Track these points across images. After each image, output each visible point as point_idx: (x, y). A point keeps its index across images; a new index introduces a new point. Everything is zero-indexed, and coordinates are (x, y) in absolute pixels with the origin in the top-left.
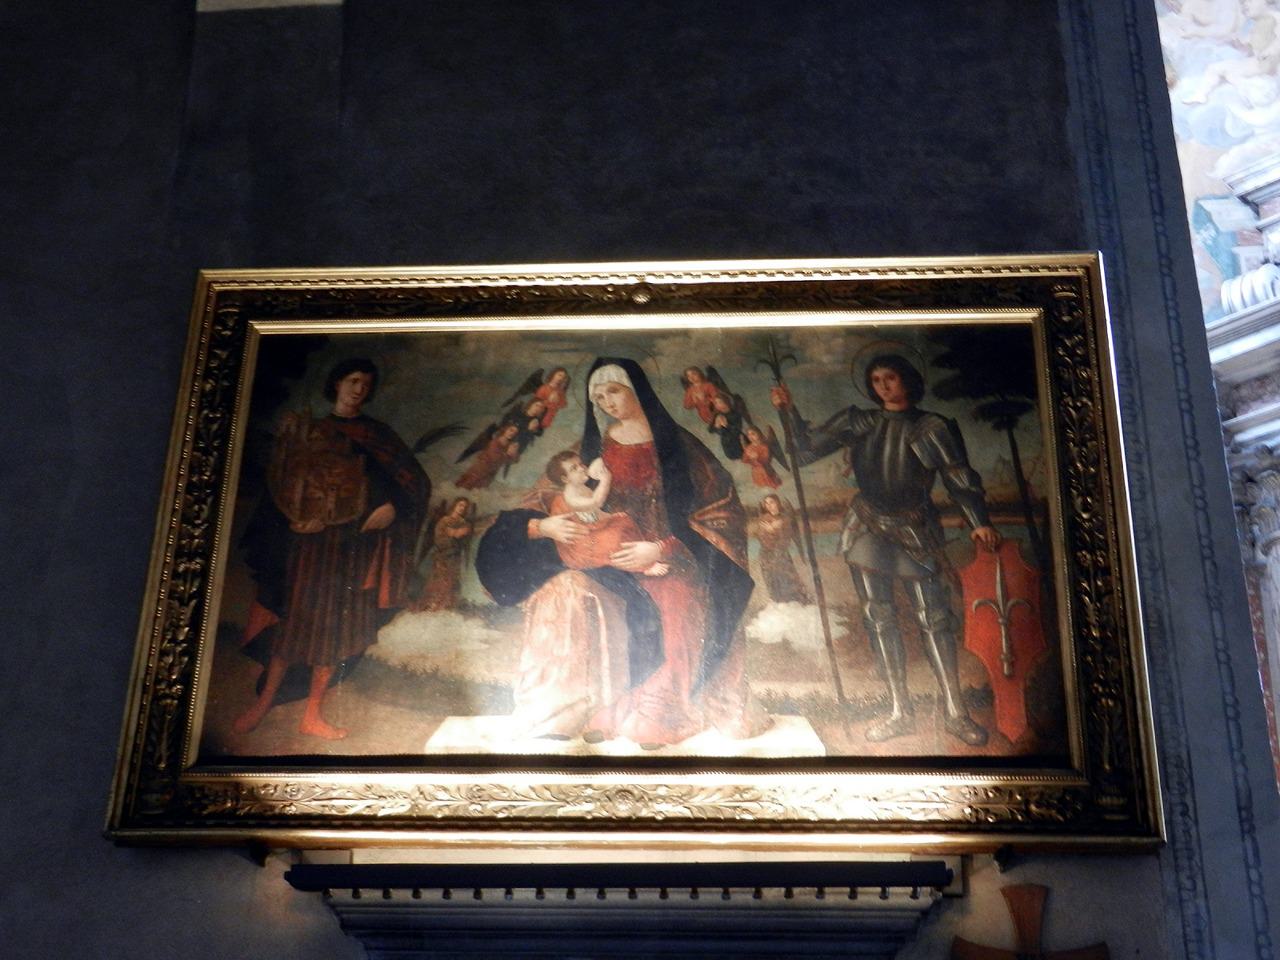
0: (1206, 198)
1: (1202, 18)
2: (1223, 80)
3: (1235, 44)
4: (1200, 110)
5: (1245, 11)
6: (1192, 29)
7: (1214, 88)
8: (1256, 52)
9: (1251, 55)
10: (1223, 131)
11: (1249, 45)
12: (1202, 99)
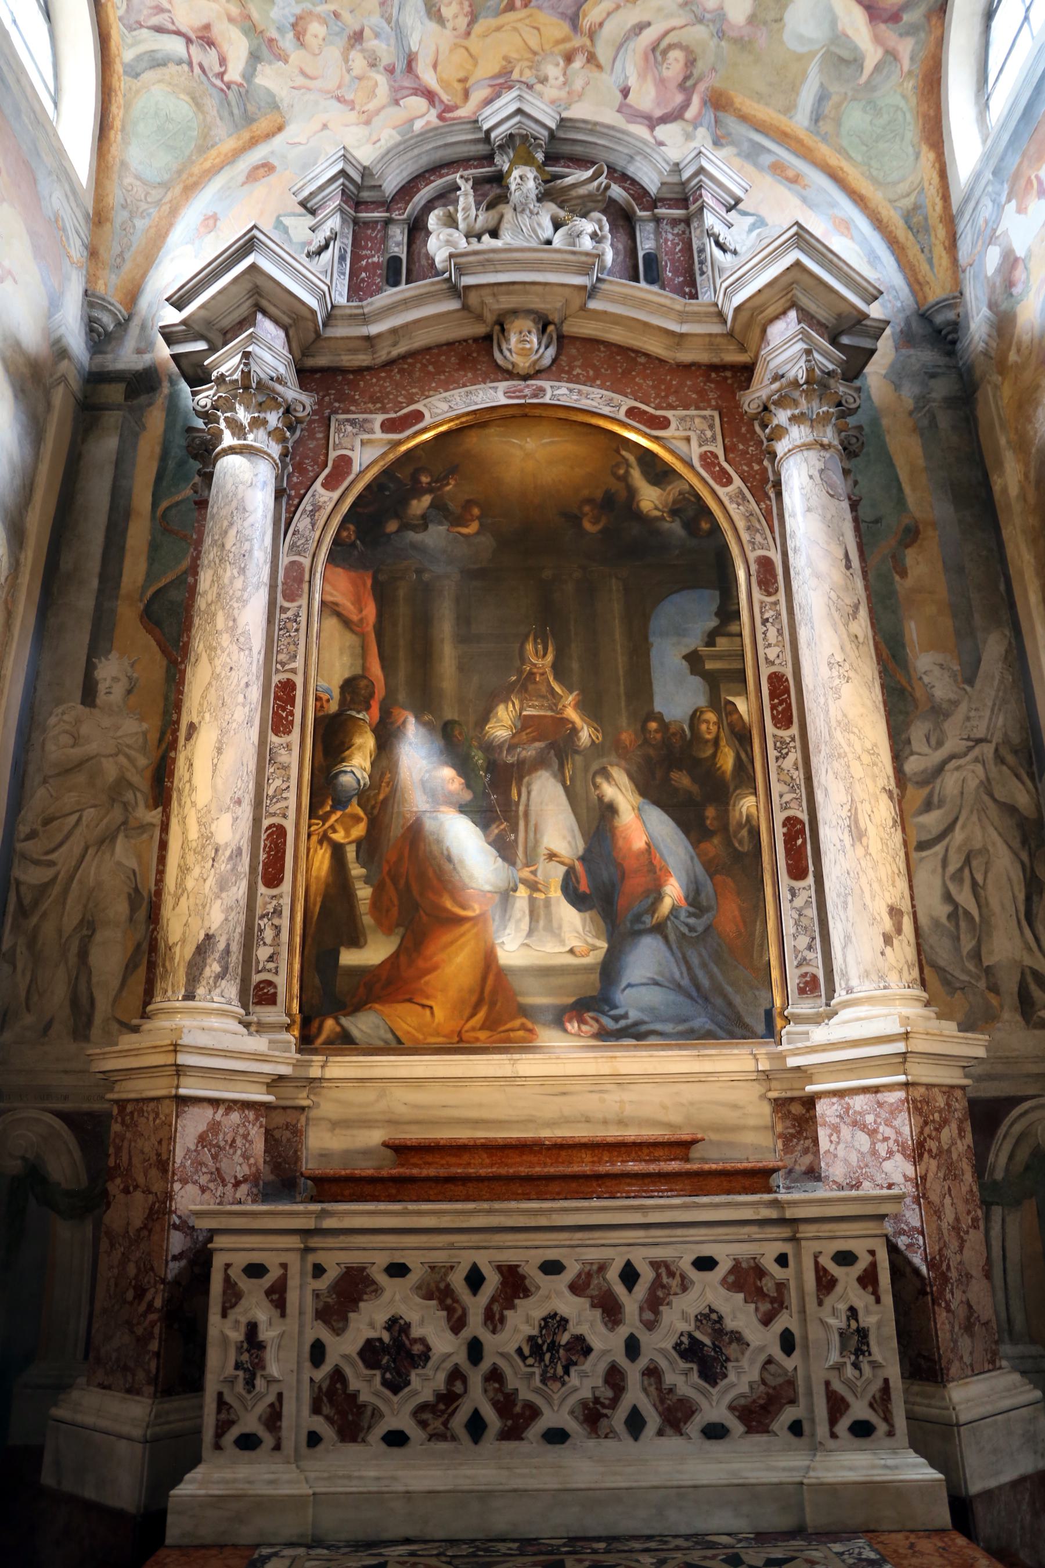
2: (325, 126)
3: (340, 99)
5: (349, 71)
6: (300, 81)
7: (316, 133)
8: (357, 107)
9: (353, 109)
11: (353, 102)
12: (304, 141)
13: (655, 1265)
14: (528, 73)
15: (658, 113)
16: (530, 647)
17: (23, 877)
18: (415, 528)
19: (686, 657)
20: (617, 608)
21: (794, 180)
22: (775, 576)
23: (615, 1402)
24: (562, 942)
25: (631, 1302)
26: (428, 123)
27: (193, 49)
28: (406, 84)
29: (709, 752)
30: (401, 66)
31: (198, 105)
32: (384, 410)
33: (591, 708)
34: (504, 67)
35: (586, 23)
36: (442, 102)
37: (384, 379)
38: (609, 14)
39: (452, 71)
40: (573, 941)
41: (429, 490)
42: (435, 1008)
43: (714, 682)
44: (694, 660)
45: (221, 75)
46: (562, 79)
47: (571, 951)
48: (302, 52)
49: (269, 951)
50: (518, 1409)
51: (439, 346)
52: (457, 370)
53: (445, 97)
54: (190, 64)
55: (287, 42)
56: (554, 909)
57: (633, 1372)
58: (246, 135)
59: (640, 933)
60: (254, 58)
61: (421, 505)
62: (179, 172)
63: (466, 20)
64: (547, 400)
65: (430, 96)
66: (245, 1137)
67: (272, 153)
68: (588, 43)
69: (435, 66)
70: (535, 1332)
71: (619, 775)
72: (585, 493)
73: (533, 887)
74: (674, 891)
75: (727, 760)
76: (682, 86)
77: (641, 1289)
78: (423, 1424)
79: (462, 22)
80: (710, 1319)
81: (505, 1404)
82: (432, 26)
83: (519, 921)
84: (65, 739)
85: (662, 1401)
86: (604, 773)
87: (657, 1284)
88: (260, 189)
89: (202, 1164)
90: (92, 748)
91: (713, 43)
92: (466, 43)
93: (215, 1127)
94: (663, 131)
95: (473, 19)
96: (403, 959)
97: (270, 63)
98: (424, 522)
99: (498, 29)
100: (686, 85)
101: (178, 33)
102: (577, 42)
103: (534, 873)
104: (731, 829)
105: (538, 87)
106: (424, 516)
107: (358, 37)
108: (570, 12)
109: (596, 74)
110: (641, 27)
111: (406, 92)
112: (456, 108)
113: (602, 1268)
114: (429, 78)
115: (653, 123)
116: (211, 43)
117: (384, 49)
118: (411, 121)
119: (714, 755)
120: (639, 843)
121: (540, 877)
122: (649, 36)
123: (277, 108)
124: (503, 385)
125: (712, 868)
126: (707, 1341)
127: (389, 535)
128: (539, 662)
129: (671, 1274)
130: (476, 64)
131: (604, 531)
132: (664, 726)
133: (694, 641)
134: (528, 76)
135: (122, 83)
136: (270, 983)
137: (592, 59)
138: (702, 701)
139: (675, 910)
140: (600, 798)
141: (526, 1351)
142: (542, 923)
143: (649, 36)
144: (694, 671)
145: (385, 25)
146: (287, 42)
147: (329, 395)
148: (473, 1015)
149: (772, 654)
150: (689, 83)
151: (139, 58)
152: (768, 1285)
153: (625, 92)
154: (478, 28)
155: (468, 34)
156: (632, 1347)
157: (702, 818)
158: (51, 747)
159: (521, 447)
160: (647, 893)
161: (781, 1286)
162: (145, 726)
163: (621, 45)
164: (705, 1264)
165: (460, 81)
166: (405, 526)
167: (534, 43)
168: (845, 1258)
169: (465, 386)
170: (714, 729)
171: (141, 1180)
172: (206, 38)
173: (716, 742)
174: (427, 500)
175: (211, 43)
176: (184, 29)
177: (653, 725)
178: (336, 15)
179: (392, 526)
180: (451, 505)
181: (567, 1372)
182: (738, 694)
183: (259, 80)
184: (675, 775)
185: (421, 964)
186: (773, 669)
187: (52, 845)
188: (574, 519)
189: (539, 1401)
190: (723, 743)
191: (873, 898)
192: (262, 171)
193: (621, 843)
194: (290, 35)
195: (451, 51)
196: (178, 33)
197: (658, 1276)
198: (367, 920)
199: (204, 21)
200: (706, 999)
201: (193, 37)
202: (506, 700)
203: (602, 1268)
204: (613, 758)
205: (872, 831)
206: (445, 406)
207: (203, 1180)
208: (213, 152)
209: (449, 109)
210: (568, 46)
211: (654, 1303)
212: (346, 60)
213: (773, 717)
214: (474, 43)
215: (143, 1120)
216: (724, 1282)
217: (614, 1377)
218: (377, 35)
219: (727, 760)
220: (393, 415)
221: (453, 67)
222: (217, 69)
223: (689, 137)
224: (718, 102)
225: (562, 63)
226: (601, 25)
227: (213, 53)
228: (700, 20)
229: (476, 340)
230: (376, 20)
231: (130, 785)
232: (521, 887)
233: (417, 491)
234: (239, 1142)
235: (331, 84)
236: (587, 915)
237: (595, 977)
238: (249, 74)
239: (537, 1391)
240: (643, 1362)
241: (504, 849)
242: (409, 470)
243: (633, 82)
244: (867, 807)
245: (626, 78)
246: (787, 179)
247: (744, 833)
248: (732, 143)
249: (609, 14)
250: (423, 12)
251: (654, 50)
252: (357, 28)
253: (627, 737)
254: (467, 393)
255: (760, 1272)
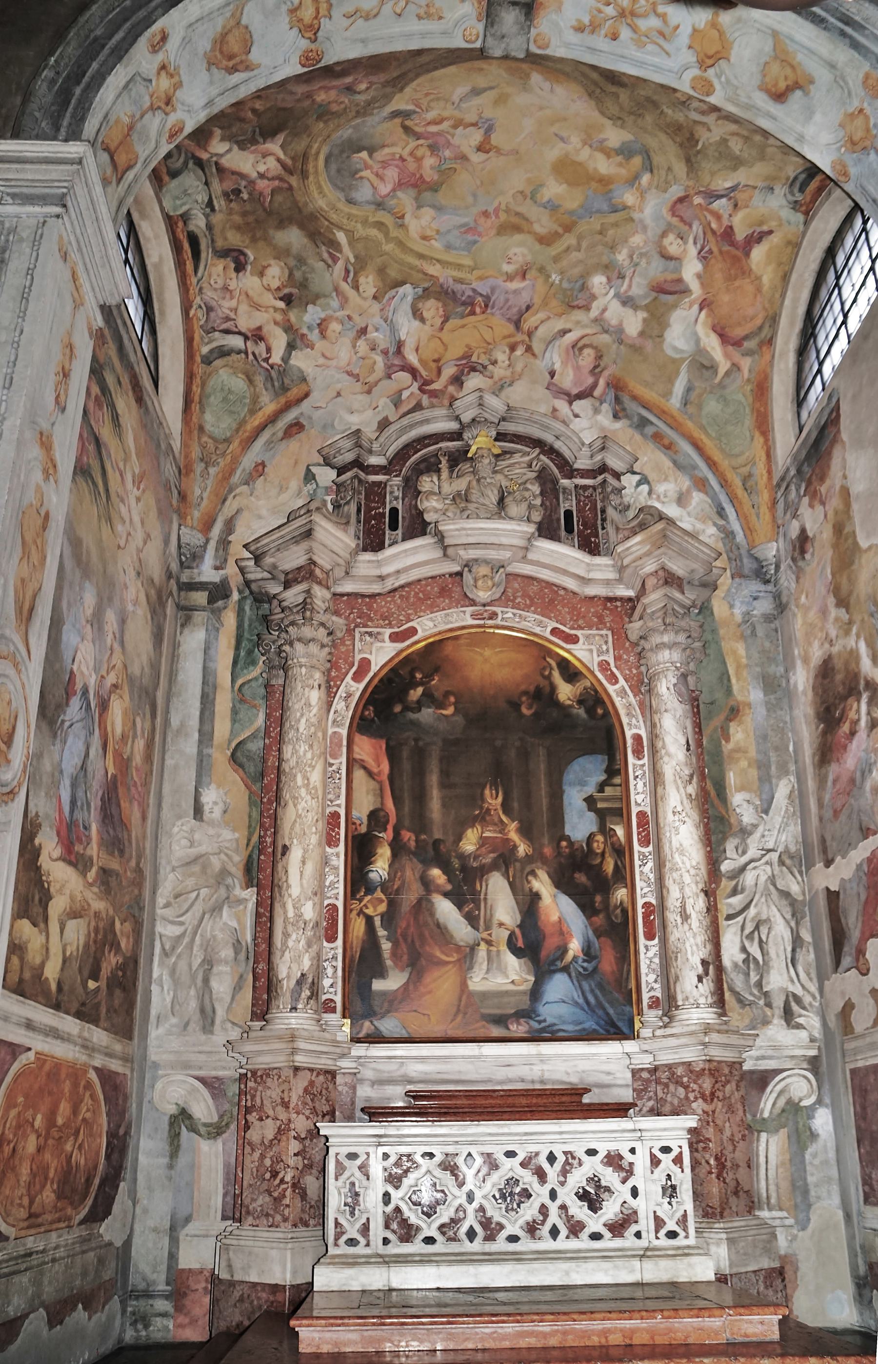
0: (314, 465)
1: (328, 354)
2: (339, 394)
3: (349, 374)
4: (321, 411)
5: (356, 353)
6: (321, 361)
10: (333, 426)
13: (565, 1153)
14: (483, 356)
15: (575, 391)
16: (487, 792)
17: (163, 932)
18: (412, 710)
19: (585, 800)
20: (542, 766)
21: (668, 447)
22: (643, 747)
23: (543, 1222)
24: (508, 978)
25: (552, 1172)
26: (412, 394)
27: (249, 343)
28: (396, 362)
29: (598, 861)
30: (392, 350)
31: (250, 381)
32: (390, 625)
33: (526, 831)
34: (466, 352)
35: (525, 327)
36: (421, 376)
37: (390, 602)
38: (542, 322)
39: (429, 353)
40: (515, 977)
41: (421, 684)
42: (432, 1017)
43: (602, 815)
44: (590, 801)
45: (266, 360)
46: (507, 362)
47: (513, 982)
48: (324, 342)
49: (330, 981)
50: (493, 1226)
51: (426, 579)
52: (438, 597)
53: (424, 373)
54: (246, 353)
55: (314, 336)
56: (502, 957)
57: (553, 1208)
58: (283, 400)
59: (554, 972)
60: (291, 347)
61: (416, 694)
62: (237, 430)
63: (440, 321)
64: (498, 621)
65: (414, 372)
66: (327, 1089)
67: (302, 414)
68: (527, 339)
69: (417, 350)
70: (502, 1187)
71: (542, 874)
72: (523, 687)
73: (489, 943)
74: (575, 946)
75: (609, 866)
76: (592, 372)
77: (558, 1165)
78: (444, 1234)
79: (438, 321)
80: (595, 1180)
81: (486, 1223)
82: (417, 323)
83: (481, 964)
84: (184, 842)
85: (568, 1221)
86: (533, 873)
87: (567, 1162)
88: (293, 445)
89: (306, 1104)
90: (203, 849)
91: (615, 346)
92: (440, 335)
93: (312, 1083)
94: (578, 405)
95: (446, 320)
96: (411, 987)
97: (301, 350)
98: (419, 706)
99: (463, 326)
100: (596, 371)
101: (240, 333)
102: (519, 337)
103: (490, 935)
104: (611, 909)
105: (490, 367)
106: (419, 702)
107: (363, 331)
108: (515, 318)
109: (531, 359)
110: (564, 332)
111: (396, 369)
112: (432, 382)
113: (537, 1154)
114: (413, 359)
115: (572, 399)
116: (261, 339)
117: (380, 337)
118: (400, 392)
119: (602, 862)
120: (554, 918)
121: (494, 938)
122: (570, 337)
123: (305, 380)
124: (469, 610)
125: (598, 933)
126: (592, 1191)
127: (396, 714)
128: (493, 802)
129: (574, 1158)
130: (446, 350)
131: (535, 714)
132: (571, 843)
133: (590, 789)
134: (484, 360)
135: (200, 369)
136: (332, 1000)
137: (529, 349)
138: (594, 829)
139: (575, 958)
140: (531, 890)
141: (498, 1196)
142: (495, 965)
143: (570, 337)
144: (590, 810)
145: (382, 322)
146: (314, 336)
147: (352, 613)
148: (453, 1020)
149: (639, 798)
150: (597, 370)
151: (212, 351)
152: (625, 1164)
153: (552, 374)
154: (449, 325)
155: (442, 329)
156: (553, 1195)
157: (593, 902)
158: (175, 847)
159: (481, 655)
160: (558, 948)
161: (631, 1164)
162: (237, 835)
163: (550, 342)
164: (592, 1152)
165: (434, 361)
166: (407, 708)
167: (488, 338)
168: (666, 1150)
169: (444, 609)
170: (602, 846)
171: (271, 1113)
172: (258, 336)
173: (603, 854)
174: (420, 690)
175: (261, 339)
176: (243, 330)
177: (564, 844)
178: (349, 318)
179: (398, 709)
180: (436, 694)
181: (519, 1206)
182: (618, 824)
183: (292, 362)
184: (577, 875)
185: (422, 989)
186: (640, 809)
187: (181, 912)
188: (515, 706)
189: (504, 1221)
190: (607, 855)
191: (693, 954)
192: (295, 429)
193: (543, 917)
194: (317, 331)
195: (429, 340)
196: (240, 333)
197: (567, 1159)
198: (389, 963)
199: (258, 324)
200: (594, 1011)
201: (250, 335)
202: (473, 826)
203: (537, 1154)
204: (539, 864)
205: (694, 916)
206: (431, 624)
207: (307, 1112)
208: (260, 414)
209: (427, 383)
210: (512, 340)
211: (564, 1172)
212: (354, 346)
213: (639, 840)
214: (445, 336)
215: (269, 1080)
216: (602, 1162)
217: (544, 1210)
218: (377, 330)
219: (609, 866)
220: (396, 630)
221: (431, 350)
222: (264, 355)
223: (596, 411)
224: (617, 386)
225: (507, 351)
226: (536, 328)
227: (262, 345)
228: (606, 332)
229: (451, 575)
230: (377, 320)
231: (230, 874)
232: (483, 944)
233: (414, 685)
234: (324, 1092)
235: (343, 363)
236: (522, 960)
237: (527, 998)
238: (286, 359)
239: (503, 1216)
240: (558, 1202)
241: (472, 920)
242: (408, 669)
243: (557, 366)
244: (691, 901)
245: (553, 364)
246: (664, 446)
247: (618, 911)
248: (627, 417)
249: (542, 322)
250: (410, 315)
251: (573, 347)
252: (364, 326)
253: (548, 851)
254: (447, 615)
255: (621, 1157)
